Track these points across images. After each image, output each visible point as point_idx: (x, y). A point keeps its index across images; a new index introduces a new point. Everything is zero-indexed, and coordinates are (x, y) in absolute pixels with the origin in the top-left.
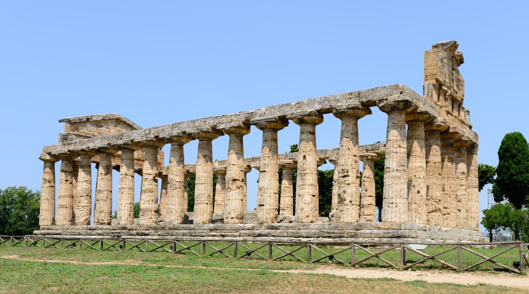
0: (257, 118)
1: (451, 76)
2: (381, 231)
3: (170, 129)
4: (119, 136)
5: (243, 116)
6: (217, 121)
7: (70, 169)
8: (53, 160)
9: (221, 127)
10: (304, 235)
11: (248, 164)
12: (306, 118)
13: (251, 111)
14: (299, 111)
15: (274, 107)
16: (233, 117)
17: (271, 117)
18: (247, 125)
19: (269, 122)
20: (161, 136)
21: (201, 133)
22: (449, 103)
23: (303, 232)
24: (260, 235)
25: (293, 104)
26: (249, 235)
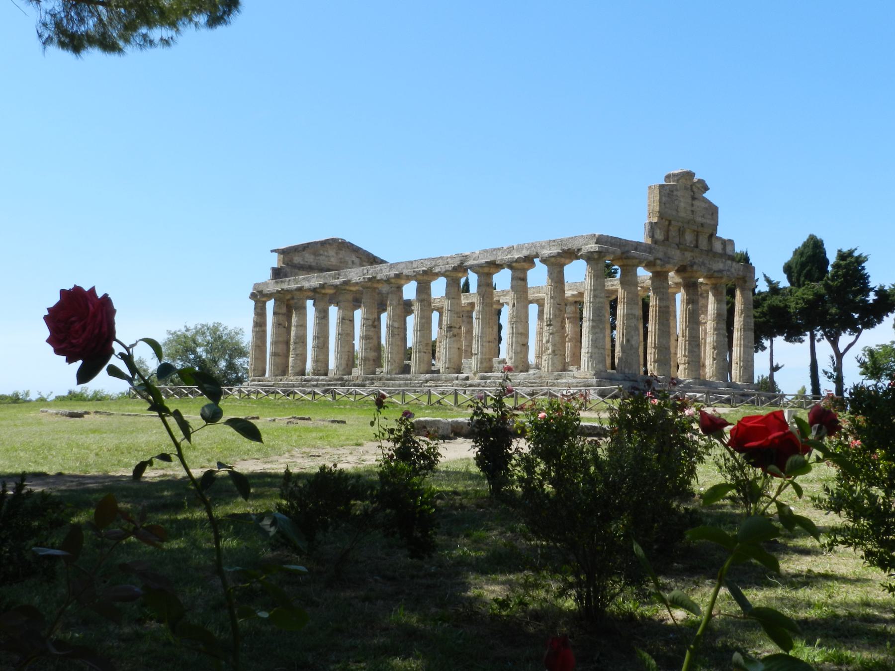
2: (574, 381)
4: (335, 274)
6: (433, 263)
7: (284, 310)
8: (264, 299)
9: (437, 270)
12: (514, 264)
14: (509, 256)
15: (486, 251)
17: (483, 261)
18: (461, 268)
19: (480, 266)
20: (378, 278)
21: (418, 277)
22: (689, 237)
24: (471, 386)
26: (461, 386)
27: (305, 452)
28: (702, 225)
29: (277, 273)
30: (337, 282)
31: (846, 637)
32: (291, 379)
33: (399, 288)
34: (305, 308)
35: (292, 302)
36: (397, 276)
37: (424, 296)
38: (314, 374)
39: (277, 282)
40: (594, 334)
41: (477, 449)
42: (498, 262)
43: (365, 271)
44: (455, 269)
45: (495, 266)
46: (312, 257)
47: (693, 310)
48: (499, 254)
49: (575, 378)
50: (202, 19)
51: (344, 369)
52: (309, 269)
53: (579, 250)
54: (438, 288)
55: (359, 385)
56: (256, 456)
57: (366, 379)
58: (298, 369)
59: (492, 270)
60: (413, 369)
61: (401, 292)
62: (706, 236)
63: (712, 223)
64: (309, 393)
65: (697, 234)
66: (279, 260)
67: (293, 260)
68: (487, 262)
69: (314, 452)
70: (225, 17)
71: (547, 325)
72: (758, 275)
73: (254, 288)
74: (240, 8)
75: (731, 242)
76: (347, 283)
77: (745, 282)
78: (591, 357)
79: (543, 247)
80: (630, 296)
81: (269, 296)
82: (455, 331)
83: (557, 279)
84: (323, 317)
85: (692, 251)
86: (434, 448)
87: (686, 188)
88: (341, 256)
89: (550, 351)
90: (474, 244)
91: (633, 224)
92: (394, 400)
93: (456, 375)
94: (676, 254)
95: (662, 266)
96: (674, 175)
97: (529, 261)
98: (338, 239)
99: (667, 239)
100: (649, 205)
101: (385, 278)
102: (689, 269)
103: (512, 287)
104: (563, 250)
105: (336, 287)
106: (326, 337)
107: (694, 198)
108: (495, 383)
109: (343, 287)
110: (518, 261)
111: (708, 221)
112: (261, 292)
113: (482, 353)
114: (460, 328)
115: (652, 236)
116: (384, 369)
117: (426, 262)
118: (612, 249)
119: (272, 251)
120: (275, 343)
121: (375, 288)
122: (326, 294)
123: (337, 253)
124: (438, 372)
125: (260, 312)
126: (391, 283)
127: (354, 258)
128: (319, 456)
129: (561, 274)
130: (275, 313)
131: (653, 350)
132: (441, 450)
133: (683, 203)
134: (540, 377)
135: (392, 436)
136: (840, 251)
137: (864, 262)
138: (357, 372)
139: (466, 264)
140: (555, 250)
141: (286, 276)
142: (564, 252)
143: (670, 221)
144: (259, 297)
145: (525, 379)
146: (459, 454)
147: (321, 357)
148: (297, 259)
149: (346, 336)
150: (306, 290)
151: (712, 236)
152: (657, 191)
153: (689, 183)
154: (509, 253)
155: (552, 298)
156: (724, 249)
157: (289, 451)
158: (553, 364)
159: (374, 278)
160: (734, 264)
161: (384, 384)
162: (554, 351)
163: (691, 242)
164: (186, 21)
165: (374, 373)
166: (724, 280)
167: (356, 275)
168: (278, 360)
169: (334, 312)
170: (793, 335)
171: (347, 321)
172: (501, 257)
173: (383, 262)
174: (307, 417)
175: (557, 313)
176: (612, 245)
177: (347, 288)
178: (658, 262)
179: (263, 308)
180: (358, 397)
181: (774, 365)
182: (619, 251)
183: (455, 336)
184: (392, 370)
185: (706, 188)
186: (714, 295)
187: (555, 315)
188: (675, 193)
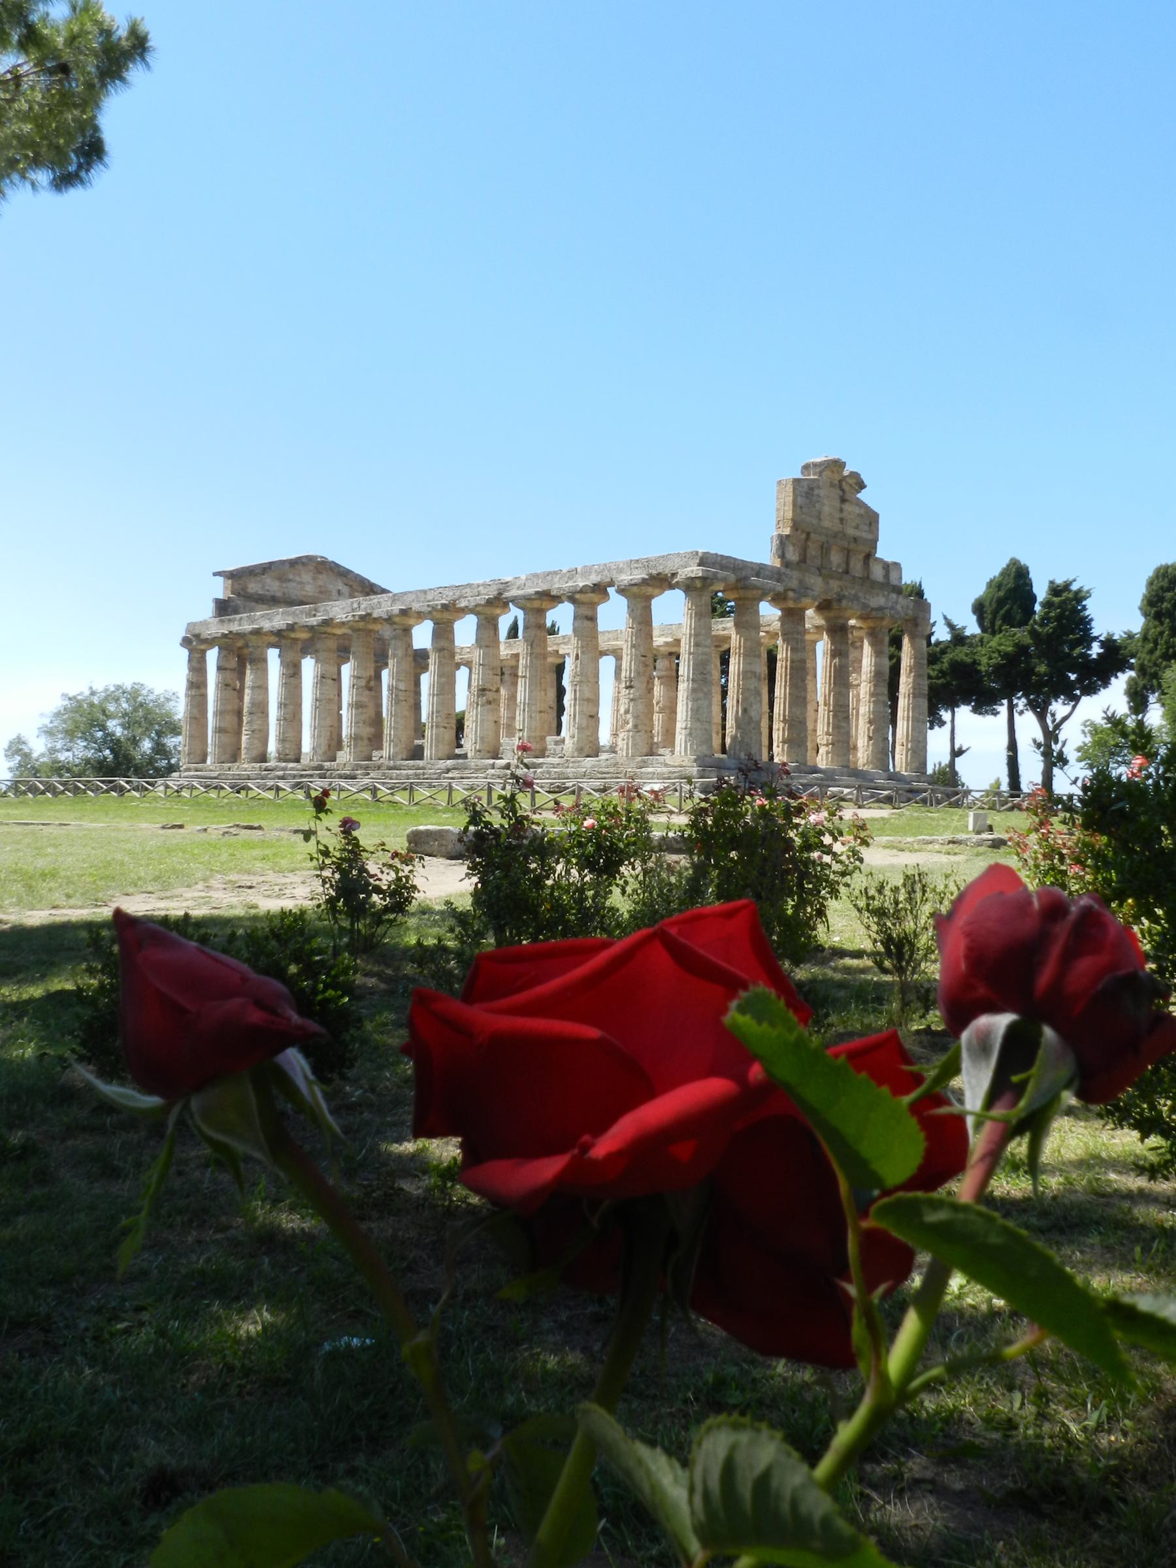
0: (514, 592)
1: (838, 515)
2: (665, 770)
3: (389, 603)
4: (310, 610)
5: (495, 587)
6: (458, 594)
7: (233, 663)
8: (202, 647)
10: (571, 775)
11: (555, 648)
12: (577, 596)
13: (508, 579)
14: (570, 584)
15: (536, 576)
16: (481, 588)
17: (531, 591)
18: (499, 601)
19: (528, 598)
20: (375, 615)
21: (435, 613)
22: (836, 558)
23: (569, 771)
25: (564, 571)
26: (499, 777)
27: (230, 881)
28: (855, 539)
29: (223, 608)
30: (313, 621)
31: (1062, 1231)
32: (245, 767)
33: (407, 631)
34: (265, 660)
35: (246, 651)
36: (404, 613)
37: (443, 643)
38: (280, 760)
39: (222, 621)
40: (694, 700)
41: (475, 879)
42: (554, 593)
43: (355, 606)
44: (489, 602)
45: (550, 598)
46: (277, 583)
47: (841, 666)
48: (556, 579)
49: (666, 765)
50: (43, 177)
51: (325, 753)
52: (272, 601)
53: (674, 575)
54: (465, 631)
55: (346, 777)
56: (150, 889)
57: (358, 767)
58: (255, 753)
59: (545, 605)
60: (427, 753)
61: (411, 637)
62: (861, 557)
63: (870, 537)
64: (270, 789)
65: (848, 554)
66: (225, 588)
67: (247, 588)
68: (537, 593)
69: (246, 880)
70: (83, 174)
71: (627, 688)
72: (935, 616)
73: (187, 630)
74: (106, 159)
75: (897, 565)
76: (327, 623)
77: (916, 625)
78: (690, 734)
79: (620, 571)
80: (748, 644)
81: (211, 642)
82: (490, 695)
83: (642, 619)
84: (292, 673)
85: (840, 579)
86: (407, 877)
87: (832, 485)
88: (320, 583)
89: (630, 726)
90: (518, 565)
91: (756, 542)
92: (397, 798)
93: (492, 761)
94: (816, 583)
95: (796, 600)
96: (815, 465)
97: (600, 590)
98: (316, 557)
99: (803, 560)
100: (778, 510)
101: (385, 616)
102: (835, 605)
103: (575, 630)
104: (651, 575)
105: (311, 628)
106: (298, 705)
107: (843, 500)
108: (549, 773)
109: (323, 629)
110: (582, 591)
111: (864, 535)
112: (197, 636)
113: (529, 728)
114: (498, 691)
115: (782, 556)
116: (385, 753)
117: (446, 592)
118: (722, 574)
119: (215, 574)
120: (219, 713)
121: (370, 631)
122: (296, 640)
123: (314, 579)
124: (465, 756)
125: (197, 667)
126: (395, 623)
127: (341, 586)
128: (250, 887)
129: (648, 609)
130: (219, 668)
131: (782, 725)
132: (417, 881)
133: (828, 505)
134: (616, 764)
135: (327, 861)
136: (1052, 582)
137: (1085, 598)
138: (345, 756)
139: (506, 595)
140: (639, 575)
141: (236, 612)
142: (652, 577)
143: (808, 534)
144: (195, 644)
145: (593, 766)
146: (446, 884)
147: (290, 735)
148: (253, 587)
149: (328, 703)
150: (266, 634)
151: (869, 556)
152: (790, 488)
153: (837, 477)
154: (570, 578)
155: (633, 646)
156: (887, 576)
157: (205, 880)
158: (634, 745)
159: (369, 615)
160: (901, 599)
161: (384, 774)
162: (635, 726)
163: (839, 566)
164: (16, 177)
165: (370, 759)
166: (885, 623)
167: (341, 610)
168: (227, 739)
169: (309, 667)
170: (984, 703)
171: (329, 680)
172: (558, 585)
173: (384, 591)
174: (256, 825)
175: (641, 669)
176: (723, 567)
177: (329, 630)
178: (791, 594)
179: (202, 660)
180: (343, 795)
181: (957, 747)
182: (732, 578)
183: (490, 703)
184: (396, 754)
185: (861, 486)
186: (872, 644)
187: (638, 673)
188: (816, 492)
